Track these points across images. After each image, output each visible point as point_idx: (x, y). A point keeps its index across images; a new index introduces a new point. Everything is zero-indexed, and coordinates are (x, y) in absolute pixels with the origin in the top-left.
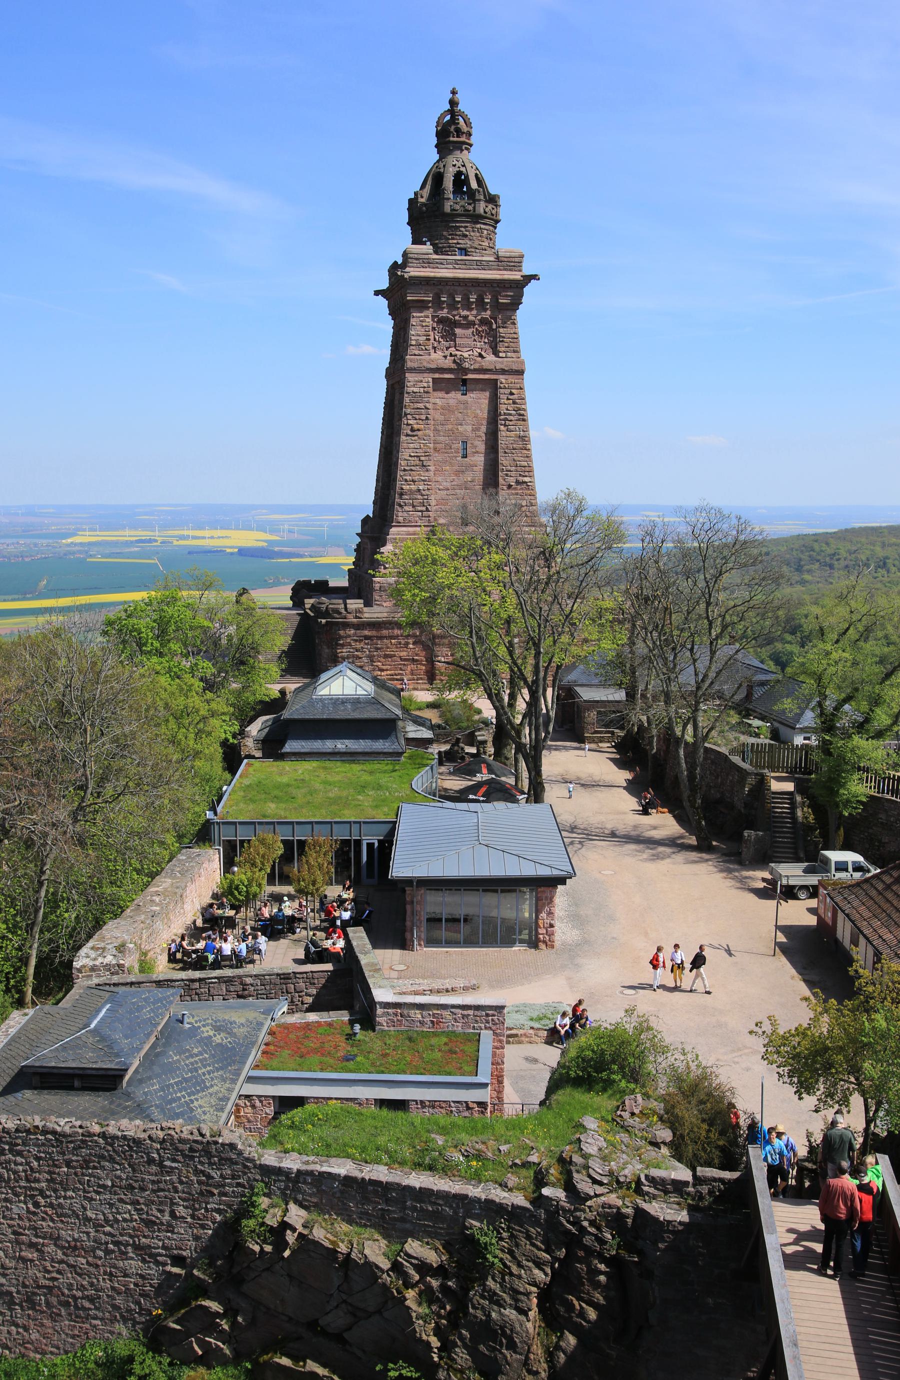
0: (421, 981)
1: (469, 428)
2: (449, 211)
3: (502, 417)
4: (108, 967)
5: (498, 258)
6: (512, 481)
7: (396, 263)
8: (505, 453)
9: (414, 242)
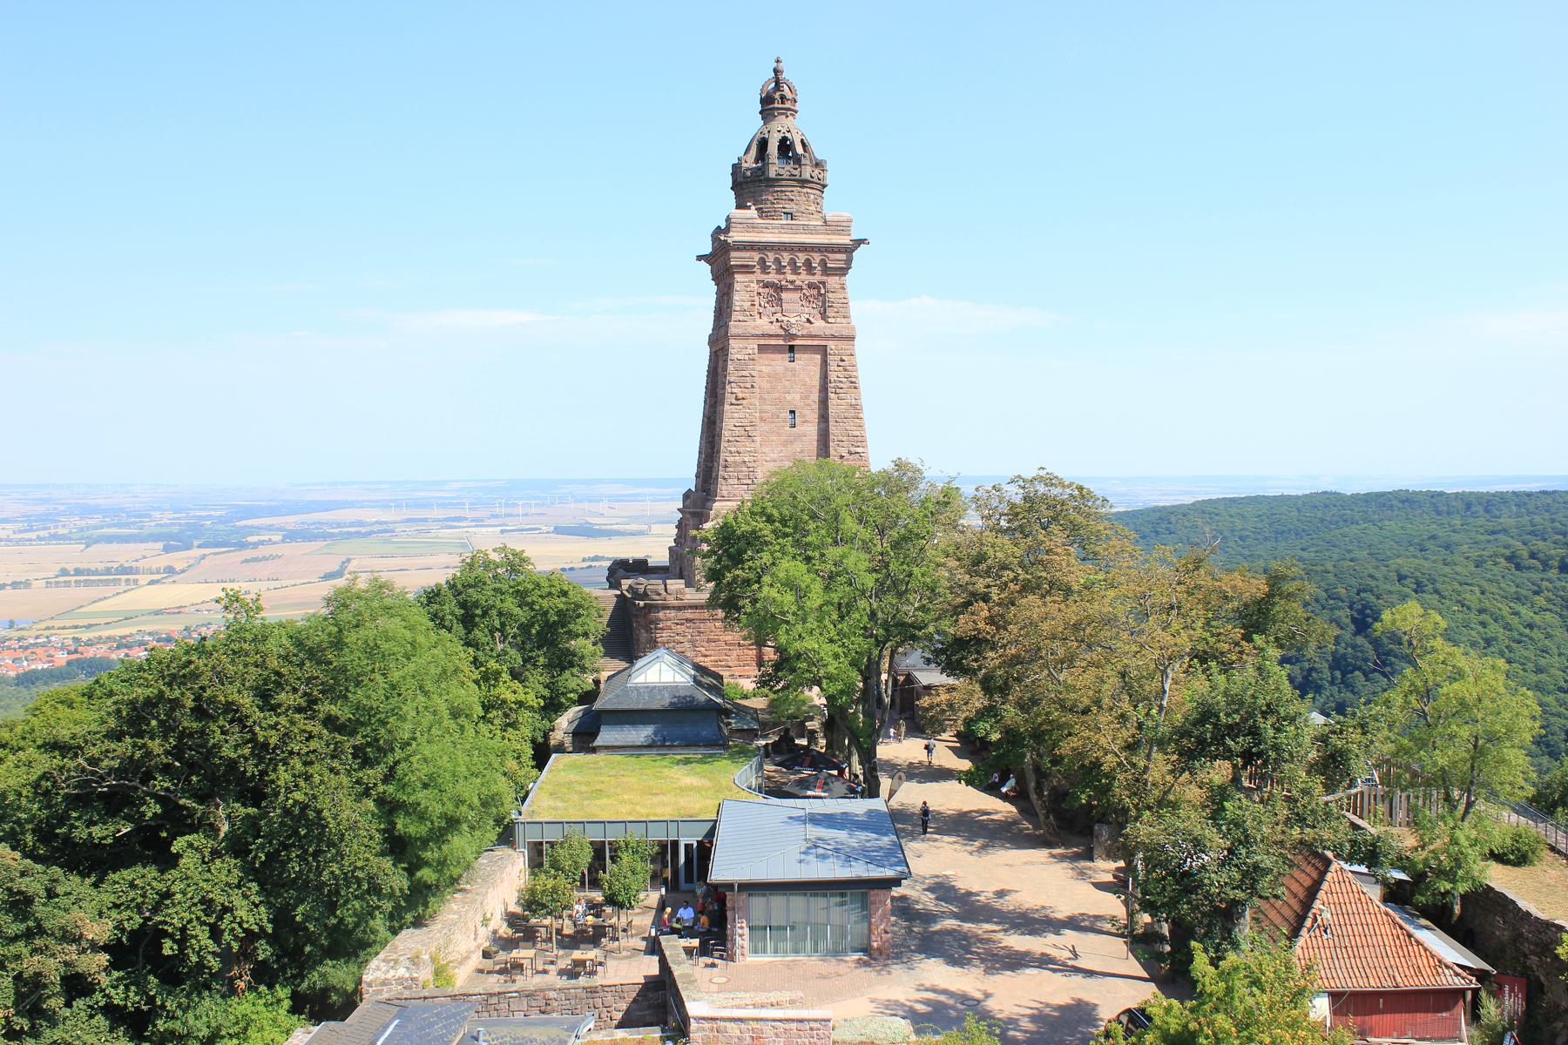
0: (742, 995)
1: (797, 397)
3: (832, 385)
4: (400, 981)
5: (825, 222)
7: (719, 227)
9: (739, 207)
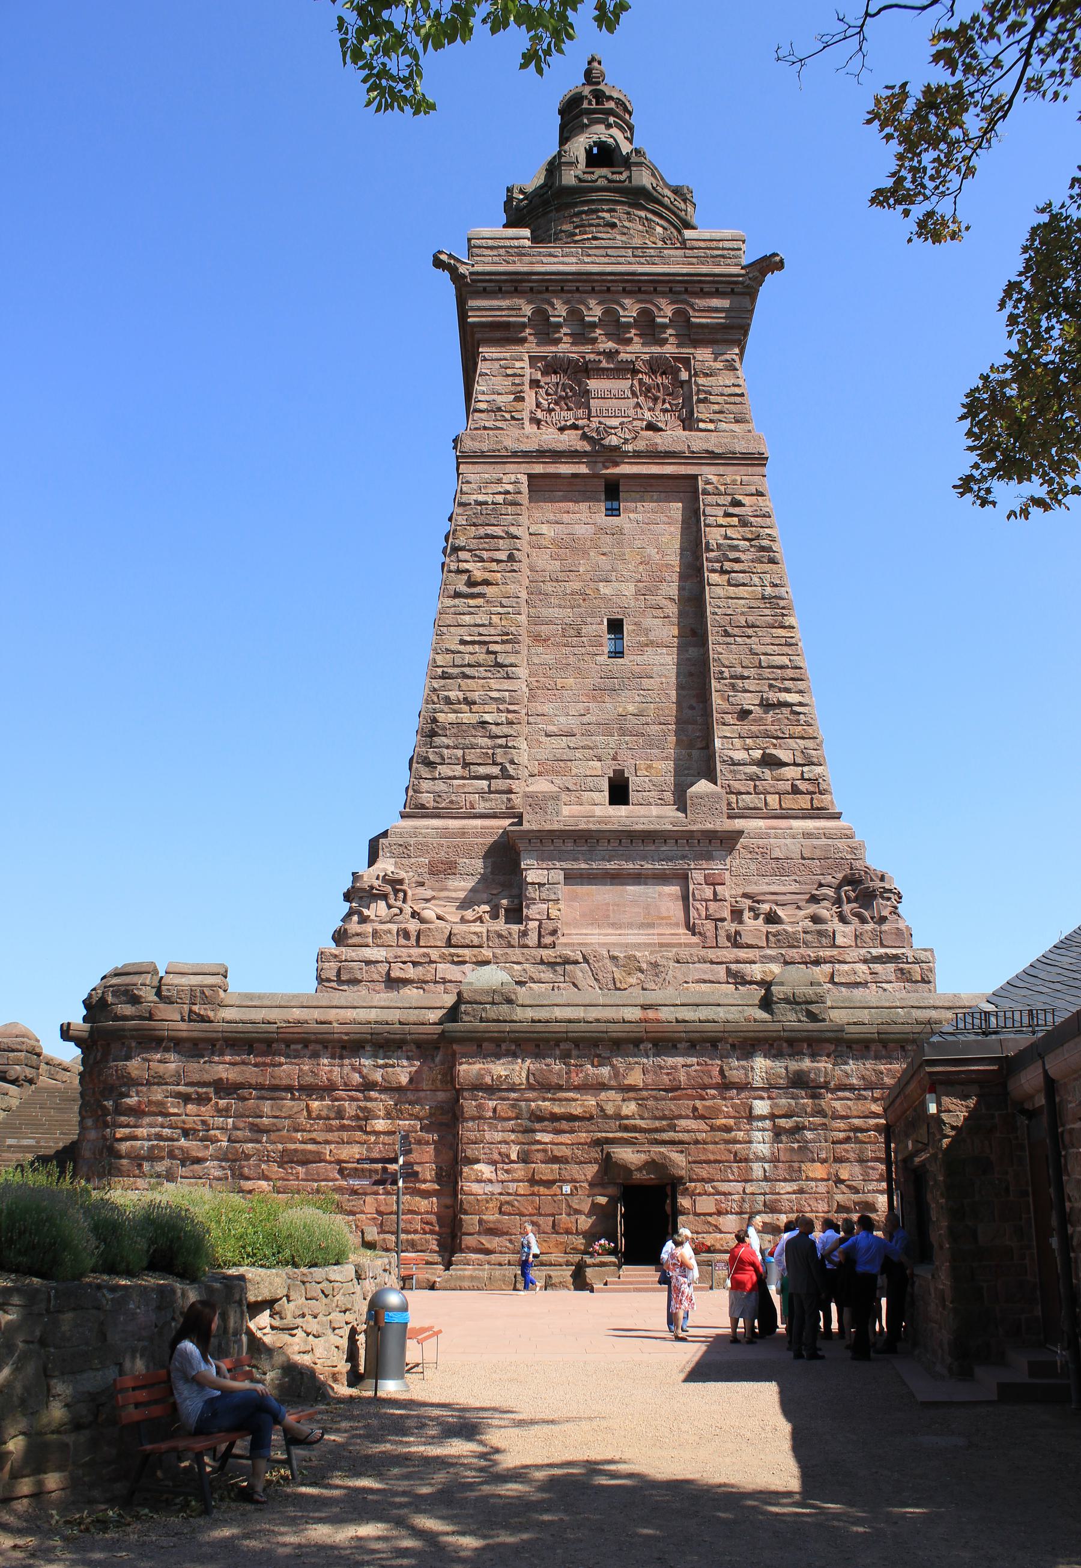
1: (629, 589)
2: (573, 182)
6: (748, 701)
8: (727, 634)
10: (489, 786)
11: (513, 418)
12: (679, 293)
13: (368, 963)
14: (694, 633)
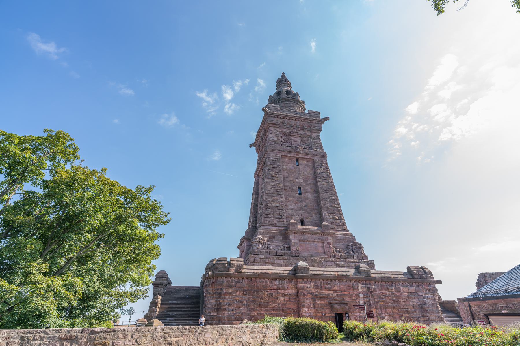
1: (302, 181)
10: (279, 220)
11: (278, 143)
12: (309, 122)
13: (260, 258)
14: (315, 191)
